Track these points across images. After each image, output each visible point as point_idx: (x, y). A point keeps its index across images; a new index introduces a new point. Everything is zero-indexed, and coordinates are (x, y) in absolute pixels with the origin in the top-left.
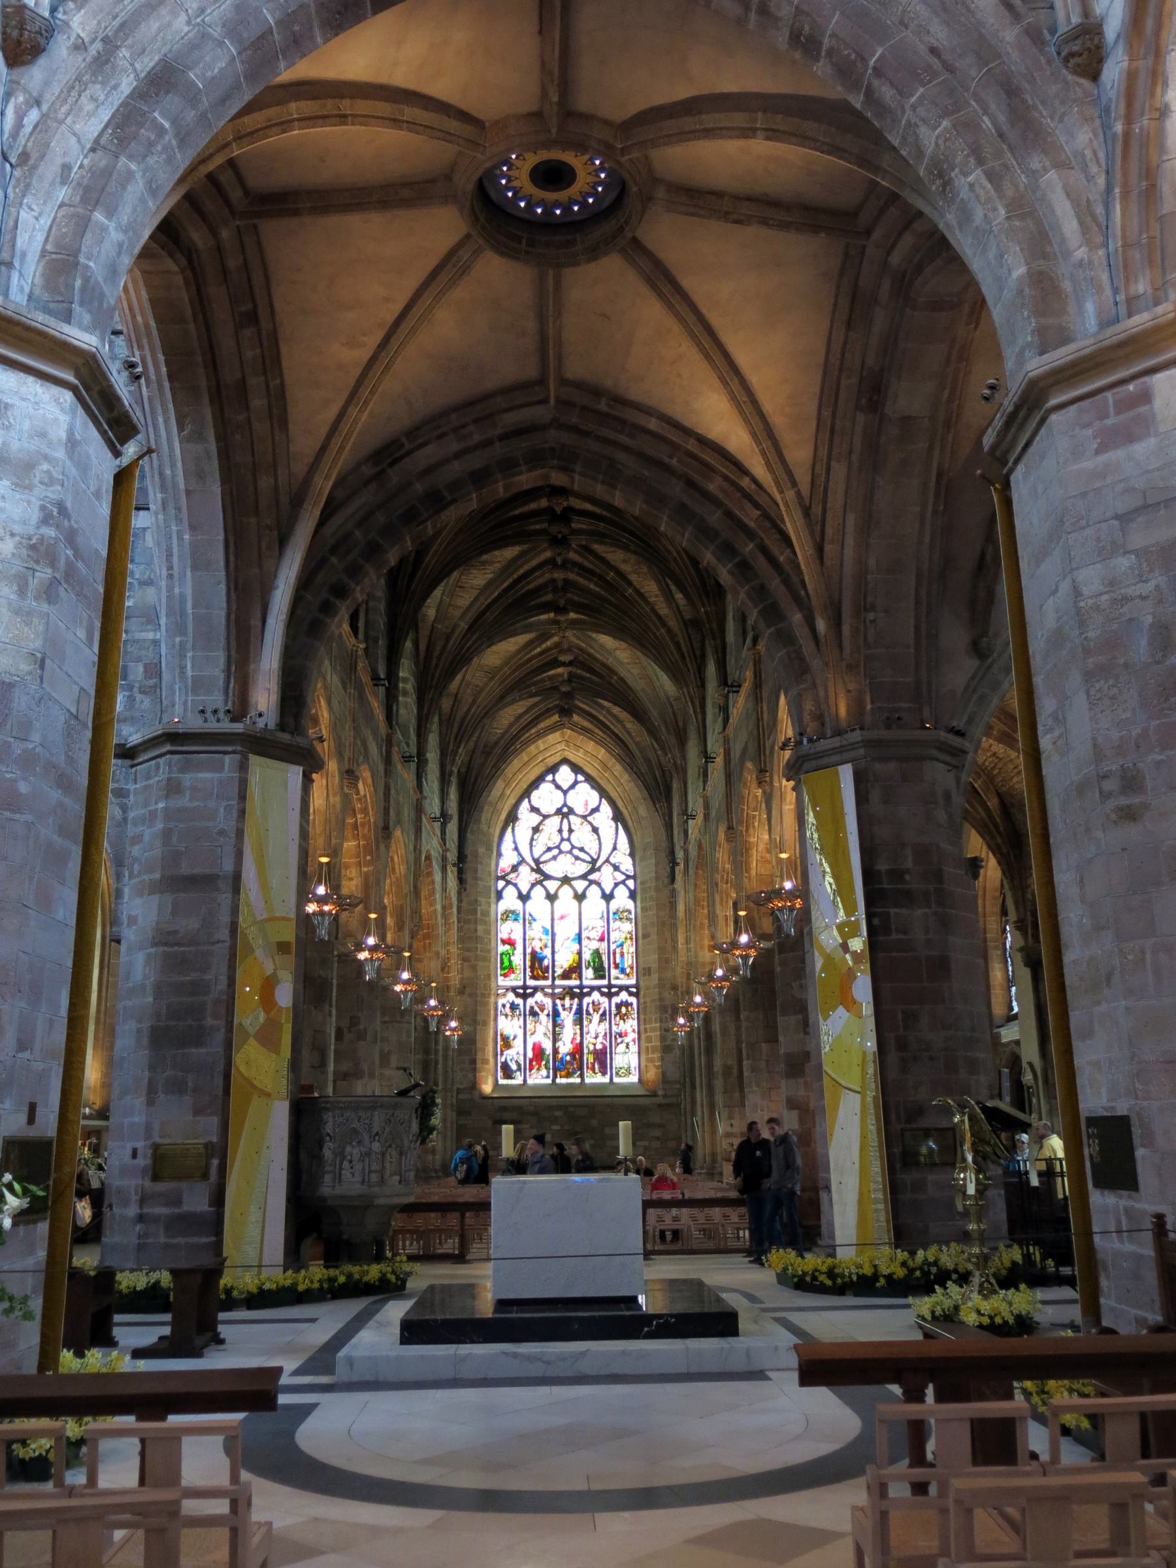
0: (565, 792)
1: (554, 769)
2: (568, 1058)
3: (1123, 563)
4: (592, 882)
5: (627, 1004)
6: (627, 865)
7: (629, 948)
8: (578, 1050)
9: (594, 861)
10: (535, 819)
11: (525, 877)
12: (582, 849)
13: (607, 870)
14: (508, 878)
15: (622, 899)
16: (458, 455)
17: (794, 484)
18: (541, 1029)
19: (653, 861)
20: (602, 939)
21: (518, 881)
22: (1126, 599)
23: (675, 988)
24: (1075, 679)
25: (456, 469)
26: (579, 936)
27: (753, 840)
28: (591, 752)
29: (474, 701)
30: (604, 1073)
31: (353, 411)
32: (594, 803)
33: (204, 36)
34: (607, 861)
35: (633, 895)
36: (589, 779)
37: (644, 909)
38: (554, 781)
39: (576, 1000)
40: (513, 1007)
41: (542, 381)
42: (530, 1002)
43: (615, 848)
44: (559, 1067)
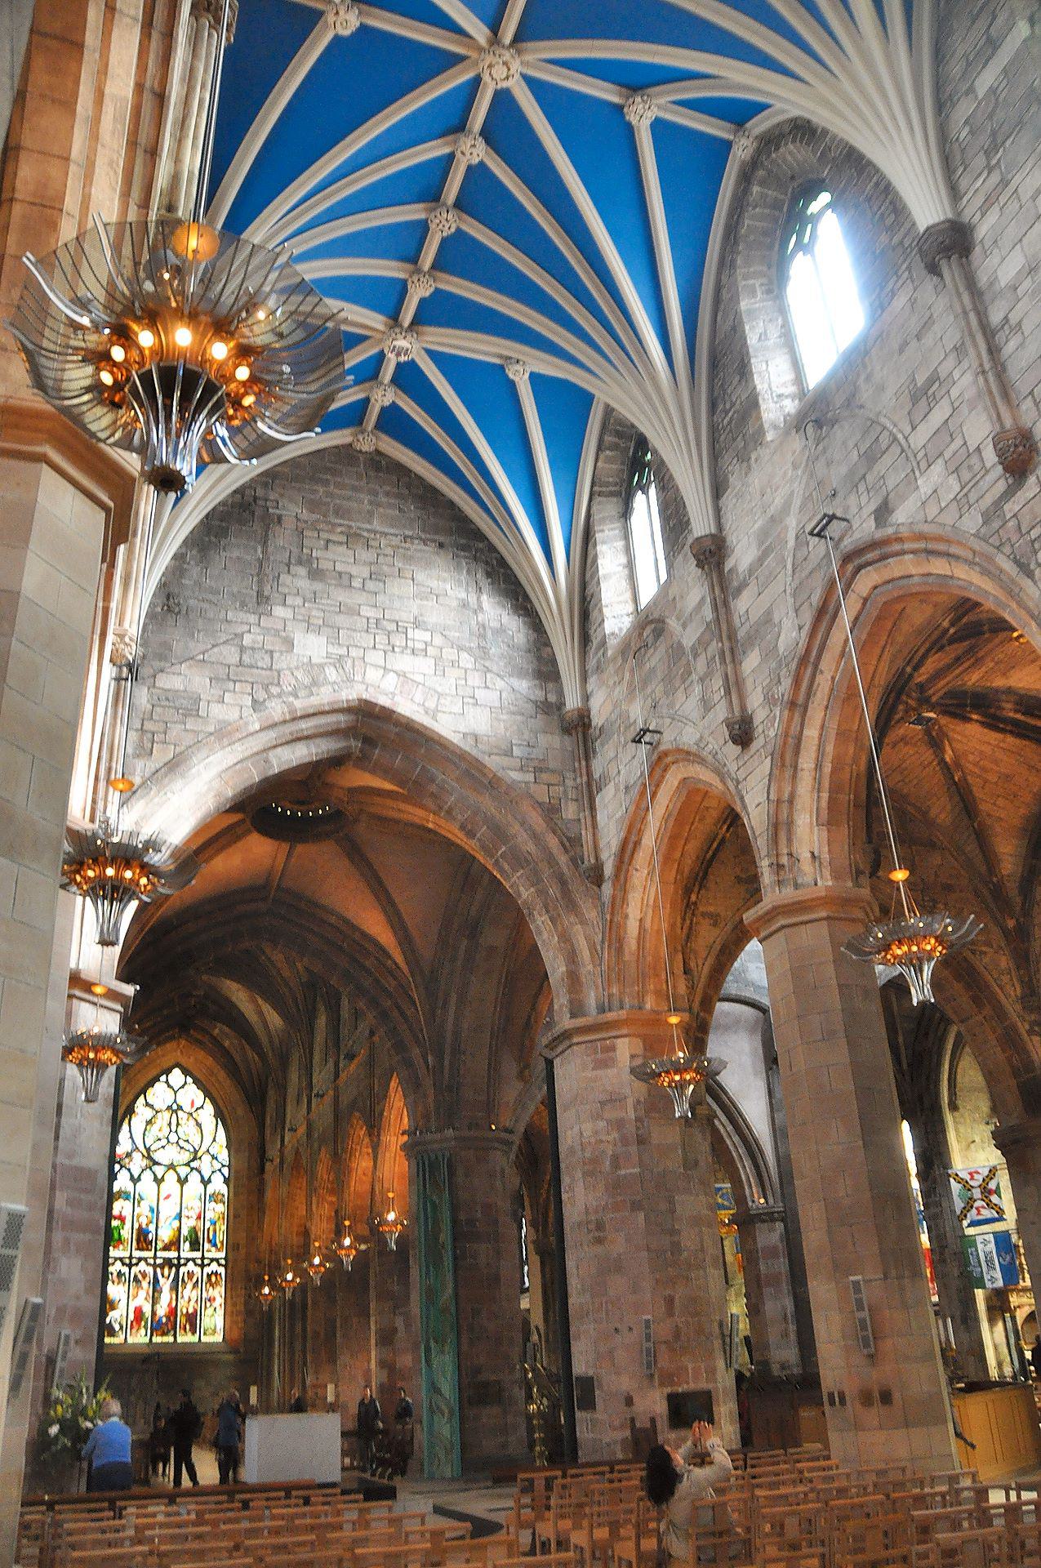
1: (168, 1072)
2: (164, 1320)
3: (602, 1124)
4: (192, 1169)
5: (216, 1274)
6: (224, 1156)
7: (222, 1227)
8: (173, 1312)
9: (196, 1152)
10: (149, 1113)
11: (137, 1163)
13: (207, 1158)
14: (123, 1163)
15: (218, 1185)
18: (142, 1294)
19: (247, 1154)
20: (199, 1217)
21: (131, 1166)
22: (602, 1141)
23: (258, 1261)
24: (579, 1174)
26: (179, 1217)
27: (354, 1165)
30: (194, 1332)
32: (198, 1104)
35: (226, 1181)
36: (196, 1082)
37: (236, 1194)
38: (167, 1082)
39: (174, 1269)
40: (120, 1274)
42: (134, 1270)
43: (214, 1140)
44: (158, 1327)
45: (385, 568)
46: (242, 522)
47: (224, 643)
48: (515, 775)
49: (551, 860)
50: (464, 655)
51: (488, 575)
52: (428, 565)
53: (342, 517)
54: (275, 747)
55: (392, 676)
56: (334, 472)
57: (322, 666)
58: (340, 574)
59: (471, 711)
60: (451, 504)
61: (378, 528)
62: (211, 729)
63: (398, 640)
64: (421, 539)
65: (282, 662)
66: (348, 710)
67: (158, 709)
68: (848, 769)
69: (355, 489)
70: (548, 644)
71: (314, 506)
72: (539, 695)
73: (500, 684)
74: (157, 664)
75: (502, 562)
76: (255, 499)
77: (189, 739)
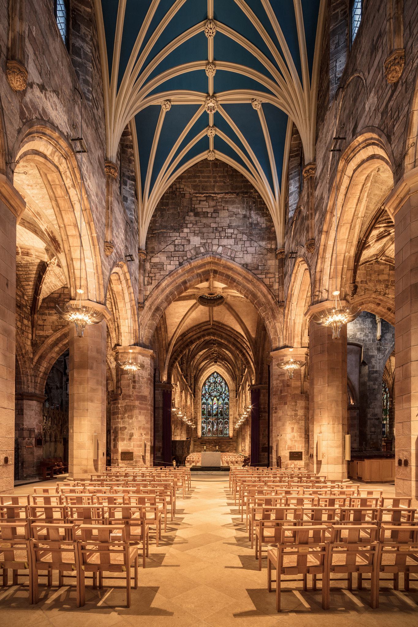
3: (278, 381)
45: (219, 207)
46: (173, 199)
48: (260, 276)
49: (269, 303)
50: (244, 236)
51: (254, 203)
52: (233, 202)
53: (205, 190)
55: (221, 248)
56: (202, 172)
57: (199, 247)
58: (204, 212)
59: (245, 256)
60: (242, 175)
61: (217, 192)
62: (167, 273)
63: (223, 234)
64: (231, 193)
67: (153, 270)
69: (209, 177)
70: (273, 226)
71: (195, 187)
72: (269, 246)
73: (256, 244)
74: (151, 255)
75: (259, 196)
76: (176, 188)
77: (162, 277)
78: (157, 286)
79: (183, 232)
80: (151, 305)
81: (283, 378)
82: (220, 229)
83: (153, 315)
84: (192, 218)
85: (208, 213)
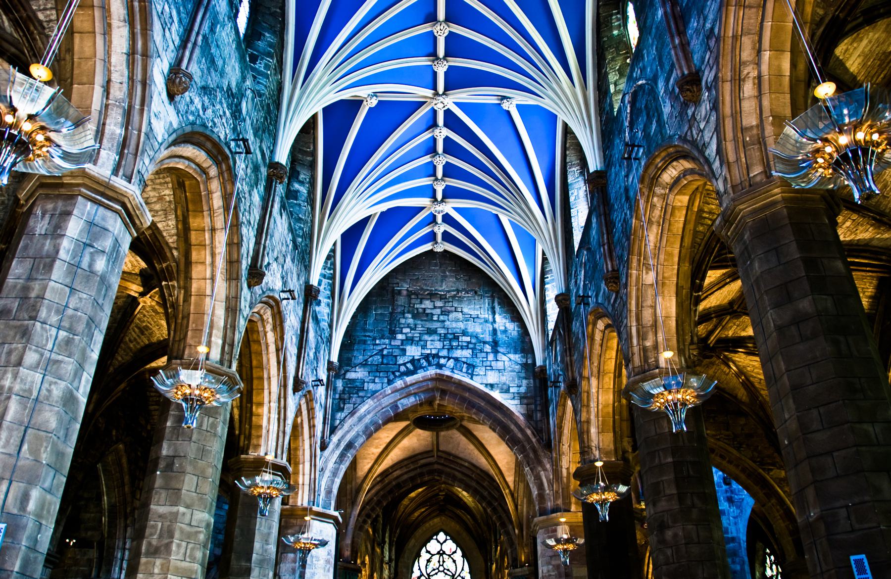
0: (442, 544)
1: (437, 534)
3: (551, 567)
10: (429, 556)
12: (448, 570)
16: (406, 473)
17: (509, 487)
22: (550, 575)
25: (406, 477)
28: (453, 525)
29: (404, 511)
31: (376, 466)
32: (454, 550)
33: (358, 434)
34: (459, 575)
38: (437, 539)
41: (432, 451)
43: (463, 570)
47: (375, 354)
54: (400, 399)
57: (419, 360)
59: (489, 373)
63: (455, 344)
65: (401, 361)
66: (431, 379)
68: (611, 406)
73: (505, 358)
78: (352, 413)
79: (395, 338)
80: (340, 441)
81: (558, 562)
82: (450, 337)
83: (342, 456)
84: (411, 321)
85: (432, 315)
